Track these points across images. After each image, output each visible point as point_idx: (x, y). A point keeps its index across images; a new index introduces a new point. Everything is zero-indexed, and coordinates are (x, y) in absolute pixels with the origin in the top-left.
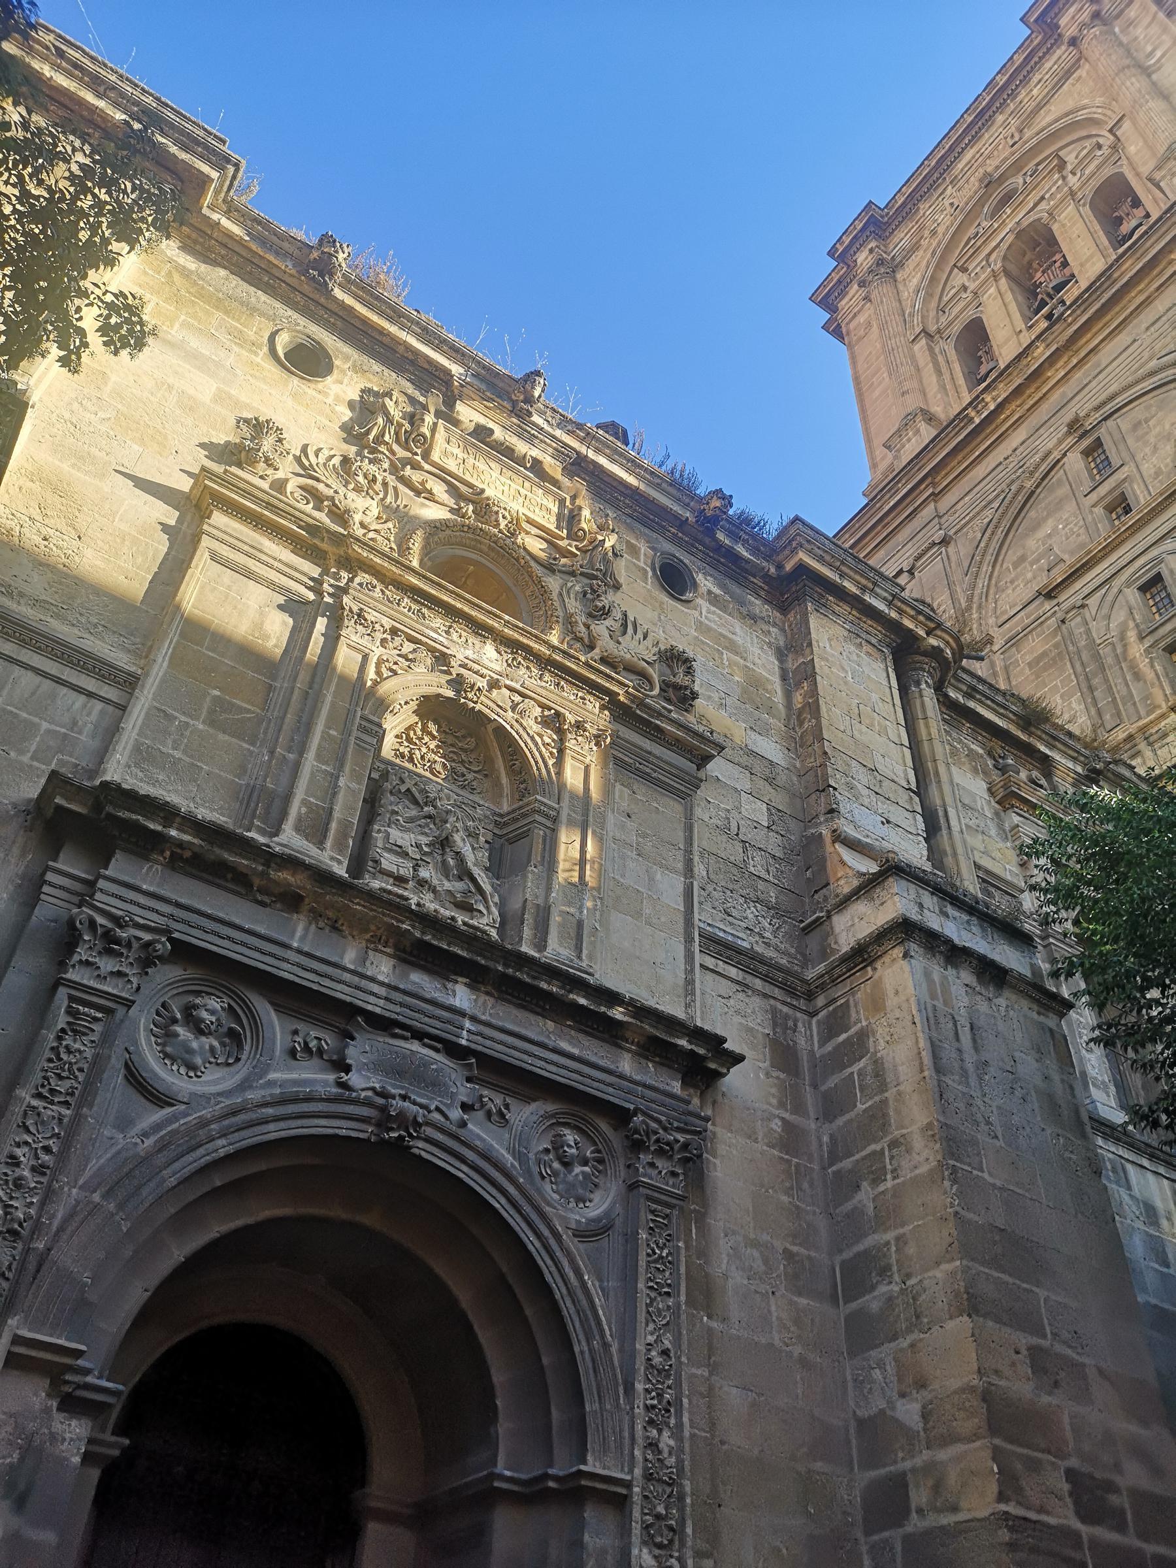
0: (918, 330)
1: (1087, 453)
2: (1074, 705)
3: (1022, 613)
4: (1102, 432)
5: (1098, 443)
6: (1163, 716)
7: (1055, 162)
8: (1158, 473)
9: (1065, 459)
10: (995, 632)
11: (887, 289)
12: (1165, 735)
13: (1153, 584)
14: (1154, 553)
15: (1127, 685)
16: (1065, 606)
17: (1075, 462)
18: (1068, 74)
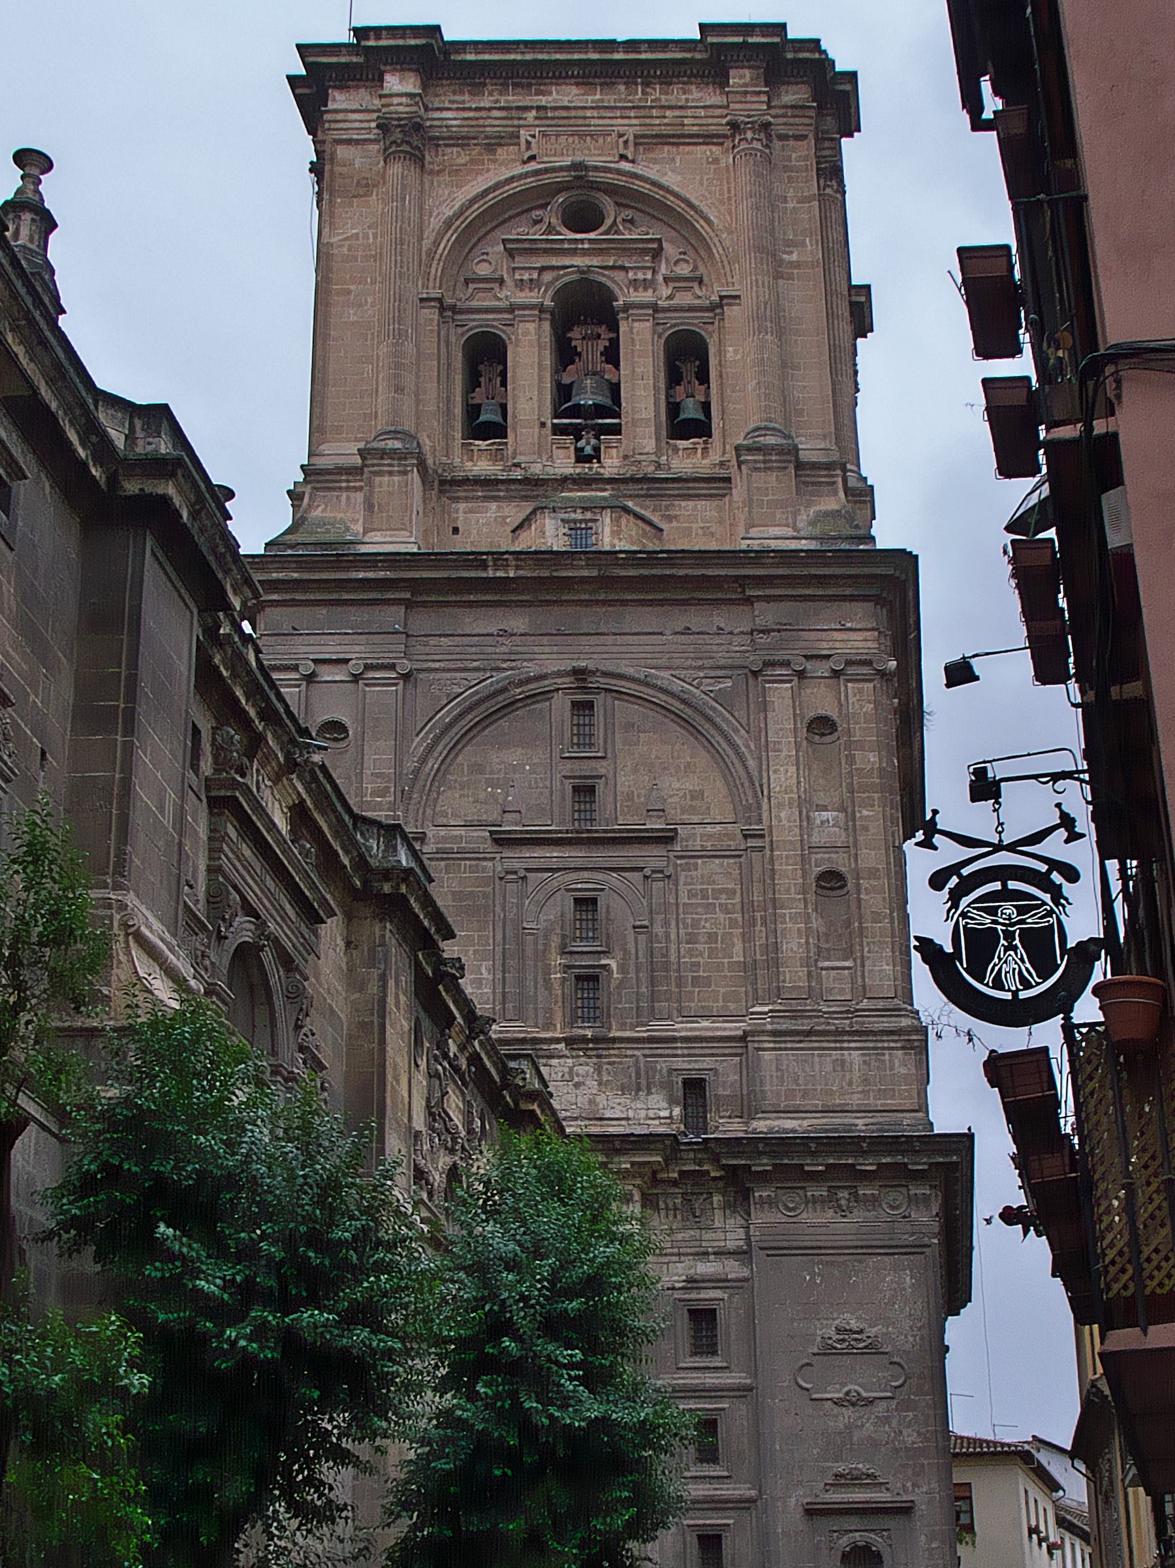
0: (435, 293)
1: (576, 705)
2: (483, 970)
3: (461, 832)
4: (599, 700)
5: (590, 705)
6: (557, 1041)
7: (655, 246)
8: (629, 796)
9: (555, 694)
10: (431, 832)
11: (413, 174)
12: (551, 1057)
13: (586, 903)
14: (599, 876)
15: (536, 988)
16: (509, 865)
17: (561, 704)
18: (708, 139)
